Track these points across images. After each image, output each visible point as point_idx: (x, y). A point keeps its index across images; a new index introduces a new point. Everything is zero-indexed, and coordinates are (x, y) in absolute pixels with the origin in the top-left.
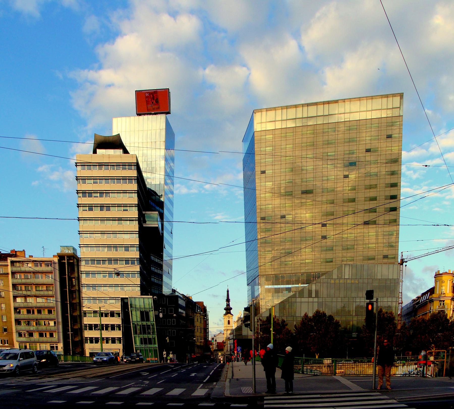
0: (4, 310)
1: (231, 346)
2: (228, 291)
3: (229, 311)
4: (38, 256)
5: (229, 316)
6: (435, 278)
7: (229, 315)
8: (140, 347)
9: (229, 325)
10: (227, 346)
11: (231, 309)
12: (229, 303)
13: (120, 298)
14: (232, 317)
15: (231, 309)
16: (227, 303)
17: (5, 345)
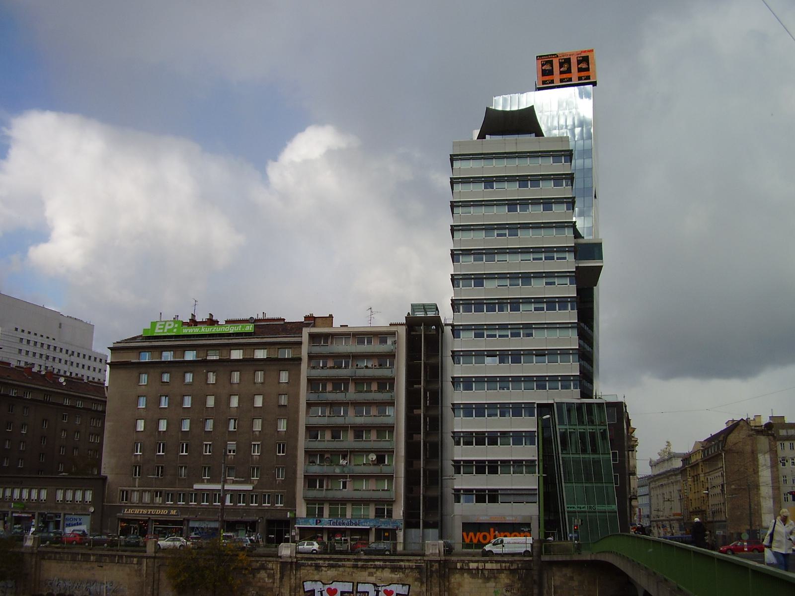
8: (579, 509)
13: (536, 406)
17: (276, 505)
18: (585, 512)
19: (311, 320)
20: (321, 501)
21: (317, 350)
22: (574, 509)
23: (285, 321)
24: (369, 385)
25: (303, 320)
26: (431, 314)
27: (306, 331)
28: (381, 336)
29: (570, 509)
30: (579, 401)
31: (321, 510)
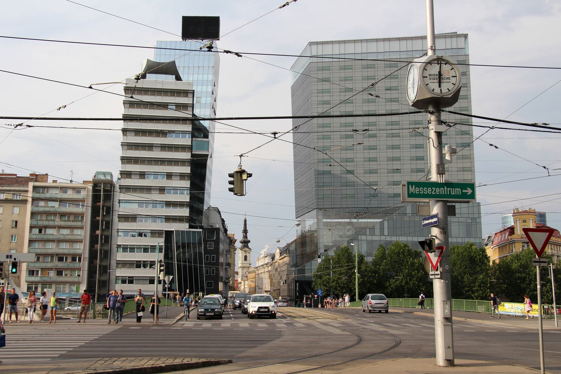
0: (14, 242)
2: (245, 221)
3: (246, 244)
4: (63, 181)
6: (513, 216)
7: (246, 249)
9: (246, 262)
11: (249, 242)
12: (246, 235)
14: (249, 252)
15: (249, 242)
19: (35, 177)
20: (37, 283)
21: (37, 195)
23: (17, 176)
24: (69, 217)
25: (28, 176)
26: (109, 178)
27: (31, 185)
28: (77, 190)
31: (36, 288)
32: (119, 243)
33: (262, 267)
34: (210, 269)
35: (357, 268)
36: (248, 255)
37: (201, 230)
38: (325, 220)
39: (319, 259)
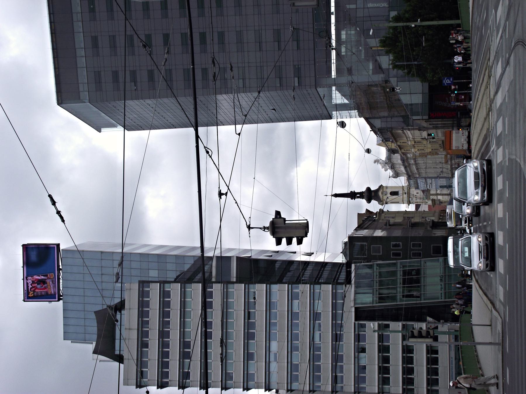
1: (441, 187)
3: (373, 193)
5: (382, 193)
7: (380, 193)
8: (443, 290)
10: (440, 195)
11: (368, 189)
13: (357, 322)
15: (368, 189)
16: (358, 197)
18: (445, 284)
22: (443, 293)
29: (443, 297)
30: (353, 286)
32: (375, 390)
33: (408, 168)
34: (413, 250)
35: (408, 24)
36: (389, 191)
37: (353, 266)
38: (334, 74)
39: (395, 89)
